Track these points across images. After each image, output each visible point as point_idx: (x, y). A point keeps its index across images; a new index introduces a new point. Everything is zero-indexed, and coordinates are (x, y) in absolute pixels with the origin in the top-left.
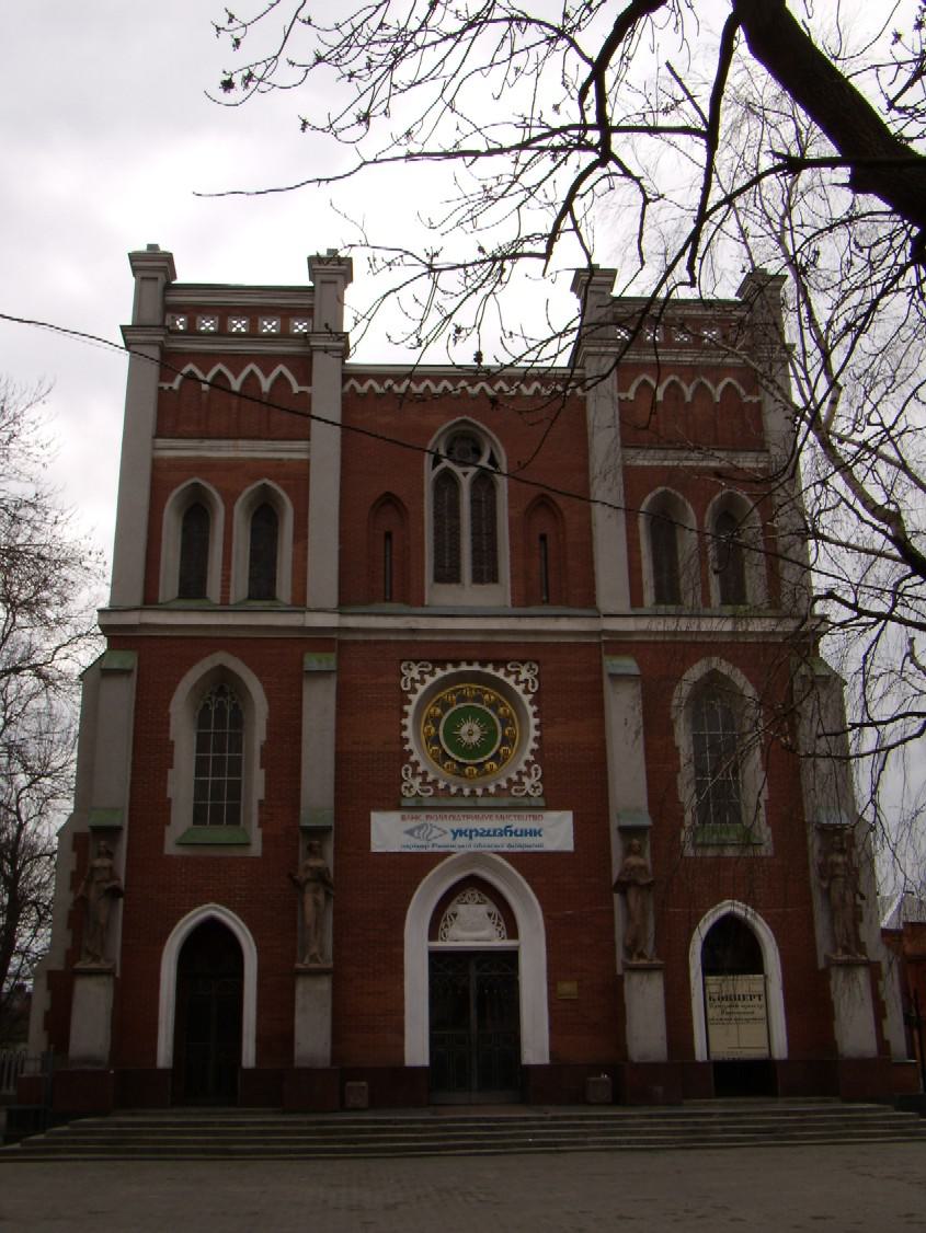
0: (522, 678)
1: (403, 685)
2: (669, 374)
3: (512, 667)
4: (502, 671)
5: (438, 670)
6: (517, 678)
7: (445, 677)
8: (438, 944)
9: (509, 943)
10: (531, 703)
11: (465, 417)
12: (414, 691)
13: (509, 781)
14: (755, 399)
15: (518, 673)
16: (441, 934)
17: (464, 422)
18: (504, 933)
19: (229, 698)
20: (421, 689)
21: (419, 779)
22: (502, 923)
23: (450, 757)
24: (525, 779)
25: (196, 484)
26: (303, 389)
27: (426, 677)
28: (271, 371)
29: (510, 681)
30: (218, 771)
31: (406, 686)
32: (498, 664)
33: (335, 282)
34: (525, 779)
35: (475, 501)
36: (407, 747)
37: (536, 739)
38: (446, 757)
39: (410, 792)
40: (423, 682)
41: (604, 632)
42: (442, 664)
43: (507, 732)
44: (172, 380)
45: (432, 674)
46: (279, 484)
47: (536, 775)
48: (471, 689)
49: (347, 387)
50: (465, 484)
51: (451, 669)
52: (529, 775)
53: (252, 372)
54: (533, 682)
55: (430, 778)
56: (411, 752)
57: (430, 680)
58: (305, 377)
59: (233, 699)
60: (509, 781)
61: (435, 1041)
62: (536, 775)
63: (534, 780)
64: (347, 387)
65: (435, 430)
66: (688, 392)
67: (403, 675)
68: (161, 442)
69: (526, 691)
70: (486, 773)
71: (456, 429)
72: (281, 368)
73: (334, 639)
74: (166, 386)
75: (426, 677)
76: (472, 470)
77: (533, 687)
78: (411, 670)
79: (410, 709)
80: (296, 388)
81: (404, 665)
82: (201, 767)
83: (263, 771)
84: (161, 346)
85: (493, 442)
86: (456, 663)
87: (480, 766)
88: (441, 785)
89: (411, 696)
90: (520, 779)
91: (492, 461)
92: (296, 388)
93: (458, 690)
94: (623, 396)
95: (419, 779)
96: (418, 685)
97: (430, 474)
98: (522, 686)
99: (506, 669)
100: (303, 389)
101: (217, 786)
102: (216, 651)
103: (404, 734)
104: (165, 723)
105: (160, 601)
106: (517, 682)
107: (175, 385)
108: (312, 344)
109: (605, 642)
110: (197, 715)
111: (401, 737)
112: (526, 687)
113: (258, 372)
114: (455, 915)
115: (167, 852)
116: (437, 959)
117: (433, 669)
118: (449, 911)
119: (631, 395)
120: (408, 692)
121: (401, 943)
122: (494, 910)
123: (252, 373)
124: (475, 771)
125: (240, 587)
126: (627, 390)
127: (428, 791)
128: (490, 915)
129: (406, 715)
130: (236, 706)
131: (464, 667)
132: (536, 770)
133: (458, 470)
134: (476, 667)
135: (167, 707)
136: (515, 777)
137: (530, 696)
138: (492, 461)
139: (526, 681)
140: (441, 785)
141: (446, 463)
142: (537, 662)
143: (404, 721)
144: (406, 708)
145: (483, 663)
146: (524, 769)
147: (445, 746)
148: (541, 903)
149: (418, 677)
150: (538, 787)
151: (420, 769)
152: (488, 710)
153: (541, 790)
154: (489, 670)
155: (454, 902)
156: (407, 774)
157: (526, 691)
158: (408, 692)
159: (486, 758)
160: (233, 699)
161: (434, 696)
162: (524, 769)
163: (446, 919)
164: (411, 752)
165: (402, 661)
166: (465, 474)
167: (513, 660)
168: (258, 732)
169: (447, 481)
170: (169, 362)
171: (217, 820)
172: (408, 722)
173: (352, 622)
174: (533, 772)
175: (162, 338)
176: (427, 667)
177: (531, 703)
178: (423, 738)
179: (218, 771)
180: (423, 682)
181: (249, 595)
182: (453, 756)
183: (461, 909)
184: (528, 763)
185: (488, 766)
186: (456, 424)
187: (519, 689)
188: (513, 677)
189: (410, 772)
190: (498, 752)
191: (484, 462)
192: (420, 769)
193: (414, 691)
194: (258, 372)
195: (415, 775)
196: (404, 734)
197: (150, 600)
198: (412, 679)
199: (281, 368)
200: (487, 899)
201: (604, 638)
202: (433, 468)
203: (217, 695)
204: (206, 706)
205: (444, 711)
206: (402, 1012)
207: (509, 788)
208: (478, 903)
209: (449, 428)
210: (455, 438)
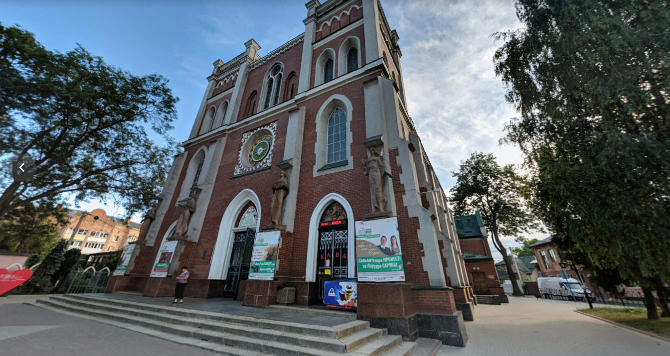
0: (273, 127)
4: (269, 127)
7: (254, 135)
8: (240, 228)
17: (276, 64)
21: (240, 169)
24: (268, 161)
32: (268, 124)
34: (268, 161)
41: (296, 101)
50: (274, 79)
52: (269, 159)
55: (242, 168)
57: (249, 136)
60: (263, 163)
63: (270, 161)
68: (209, 101)
73: (226, 133)
86: (257, 129)
88: (244, 170)
94: (317, 32)
97: (266, 80)
106: (272, 129)
116: (237, 234)
121: (218, 228)
128: (255, 216)
133: (273, 77)
138: (282, 71)
140: (244, 170)
145: (264, 126)
155: (246, 212)
157: (274, 131)
165: (243, 133)
169: (271, 81)
170: (217, 82)
184: (270, 155)
186: (274, 65)
187: (272, 131)
188: (271, 128)
191: (280, 72)
195: (239, 168)
198: (245, 138)
208: (253, 212)
209: (272, 67)
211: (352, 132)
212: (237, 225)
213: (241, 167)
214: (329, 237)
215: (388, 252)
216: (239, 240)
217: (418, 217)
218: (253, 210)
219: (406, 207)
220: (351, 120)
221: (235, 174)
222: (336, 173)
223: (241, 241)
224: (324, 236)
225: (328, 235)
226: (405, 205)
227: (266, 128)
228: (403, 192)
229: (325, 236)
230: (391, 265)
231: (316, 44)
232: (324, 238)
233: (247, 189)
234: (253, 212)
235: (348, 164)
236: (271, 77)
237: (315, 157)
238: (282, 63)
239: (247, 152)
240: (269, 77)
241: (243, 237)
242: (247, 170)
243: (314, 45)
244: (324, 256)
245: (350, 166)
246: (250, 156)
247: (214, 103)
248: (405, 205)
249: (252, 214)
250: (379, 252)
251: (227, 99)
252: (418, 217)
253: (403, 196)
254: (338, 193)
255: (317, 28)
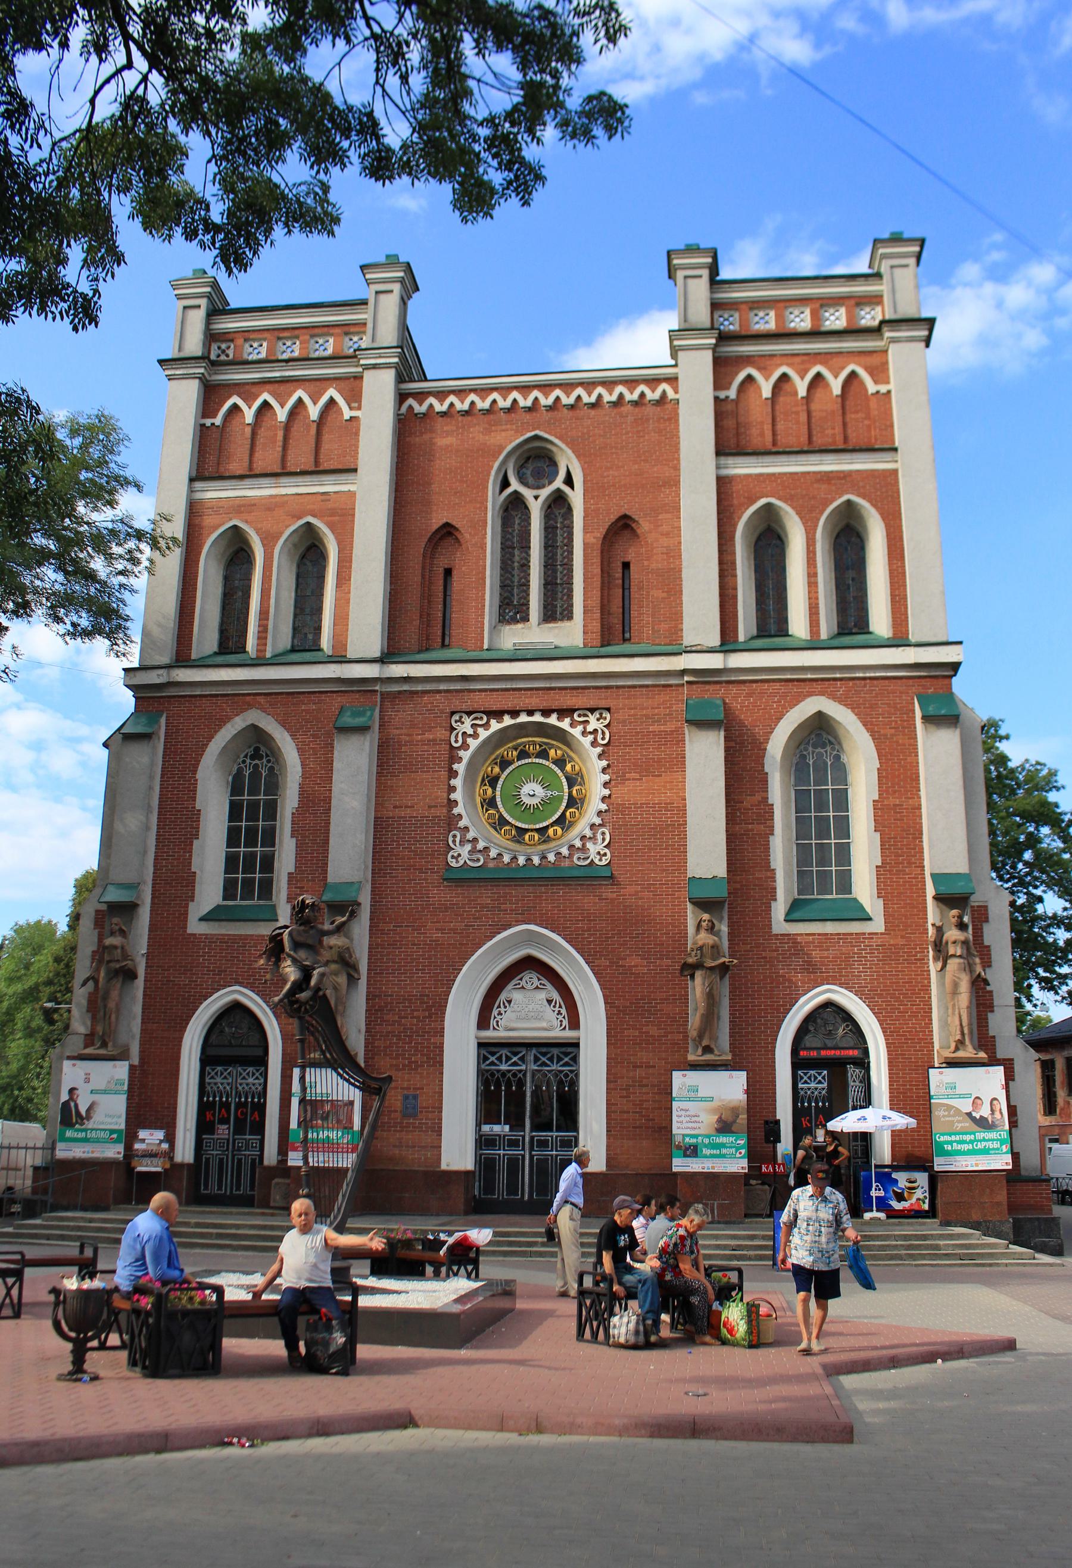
0: (590, 728)
1: (453, 739)
2: (781, 365)
3: (579, 716)
4: (567, 720)
5: (493, 722)
6: (585, 728)
8: (489, 1034)
9: (569, 1034)
10: (600, 756)
11: (537, 432)
12: (465, 746)
13: (571, 847)
14: (883, 389)
15: (587, 722)
16: (493, 1023)
17: (536, 438)
18: (565, 1023)
19: (264, 760)
20: (473, 744)
21: (468, 847)
22: (564, 1011)
23: (509, 823)
24: (589, 845)
25: (235, 527)
26: (354, 413)
27: (480, 730)
28: (319, 398)
29: (576, 732)
30: (251, 842)
31: (456, 741)
33: (392, 291)
35: (549, 530)
36: (455, 811)
37: (604, 799)
38: (503, 822)
39: (457, 862)
40: (475, 736)
42: (498, 714)
43: (574, 792)
44: (215, 416)
45: (486, 726)
46: (322, 521)
47: (604, 840)
48: (534, 743)
49: (404, 409)
51: (508, 721)
52: (593, 838)
53: (300, 400)
54: (603, 733)
55: (481, 845)
56: (460, 816)
57: (483, 734)
58: (354, 397)
59: (269, 761)
60: (571, 847)
61: (483, 1142)
62: (604, 840)
63: (600, 847)
64: (404, 409)
65: (501, 448)
66: (801, 387)
67: (453, 729)
68: (198, 485)
69: (594, 744)
70: (548, 840)
71: (526, 447)
72: (332, 392)
74: (208, 422)
75: (480, 730)
76: (545, 492)
77: (603, 739)
78: (463, 723)
79: (460, 768)
80: (347, 413)
81: (456, 717)
82: (233, 838)
83: (294, 840)
84: (202, 379)
85: (569, 459)
86: (514, 714)
87: (542, 831)
88: (493, 853)
89: (461, 753)
90: (584, 845)
91: (569, 481)
92: (347, 413)
93: (519, 745)
94: (722, 395)
95: (468, 847)
96: (469, 740)
97: (493, 501)
98: (591, 738)
99: (572, 719)
100: (354, 413)
101: (250, 858)
102: (246, 710)
103: (453, 796)
104: (191, 791)
105: (193, 657)
106: (584, 733)
107: (218, 421)
108: (362, 362)
109: (688, 682)
110: (230, 779)
111: (449, 800)
112: (595, 739)
113: (307, 400)
114: (510, 1002)
115: (189, 931)
117: (488, 722)
118: (503, 997)
119: (732, 393)
120: (459, 748)
121: (441, 1032)
122: (556, 996)
123: (300, 400)
124: (536, 838)
125: (282, 637)
126: (727, 387)
127: (478, 860)
128: (549, 1002)
129: (453, 774)
130: (272, 769)
131: (523, 718)
132: (603, 833)
133: (527, 493)
134: (538, 718)
135: (195, 772)
136: (578, 843)
137: (599, 750)
139: (596, 731)
140: (493, 853)
141: (515, 485)
142: (608, 710)
143: (453, 782)
144: (455, 766)
145: (546, 713)
146: (588, 833)
147: (502, 810)
148: (603, 987)
149: (470, 731)
150: (605, 855)
151: (470, 835)
152: (553, 767)
153: (609, 855)
154: (553, 720)
155: (510, 986)
156: (454, 842)
157: (594, 744)
158: (459, 748)
159: (551, 821)
160: (269, 761)
161: (492, 753)
162: (588, 833)
163: (499, 1006)
164: (460, 816)
165: (453, 713)
166: (536, 498)
167: (576, 710)
168: (290, 800)
169: (515, 506)
171: (248, 894)
172: (457, 782)
173: (398, 670)
174: (599, 837)
175: (202, 370)
176: (481, 718)
177: (600, 756)
178: (478, 800)
179: (251, 842)
180: (475, 736)
181: (293, 646)
182: (511, 820)
183: (517, 996)
185: (551, 831)
188: (580, 728)
189: (458, 840)
190: (563, 814)
191: (559, 483)
192: (470, 835)
193: (465, 746)
194: (307, 400)
196: (453, 796)
197: (182, 658)
198: (464, 733)
199: (332, 392)
200: (545, 981)
201: (686, 678)
202: (501, 491)
203: (253, 758)
204: (240, 772)
205: (503, 770)
206: (440, 1109)
207: (571, 856)
208: (537, 988)
210: (528, 458)
211: (878, 835)
212: (483, 1022)
213: (475, 840)
214: (820, 1082)
215: (982, 1123)
216: (492, 1064)
217: (1012, 1060)
218: (536, 983)
219: (994, 1037)
220: (876, 798)
221: (453, 864)
222: (839, 934)
223: (504, 1067)
224: (805, 1078)
225: (816, 1078)
226: (991, 1033)
227: (565, 724)
228: (991, 1008)
229: (809, 1078)
230: (990, 1145)
231: (730, 461)
232: (806, 1082)
233: (532, 927)
234: (537, 988)
235: (870, 919)
236: (515, 485)
237: (773, 879)
238: (563, 446)
239: (474, 782)
240: (505, 484)
241: (508, 1059)
242: (506, 859)
243: (723, 460)
244: (810, 1121)
245: (878, 925)
246: (491, 803)
247: (244, 507)
248: (991, 1033)
249: (542, 996)
250: (968, 1124)
251: (314, 516)
252: (1012, 1060)
253: (990, 1015)
254: (846, 988)
255: (720, 381)
